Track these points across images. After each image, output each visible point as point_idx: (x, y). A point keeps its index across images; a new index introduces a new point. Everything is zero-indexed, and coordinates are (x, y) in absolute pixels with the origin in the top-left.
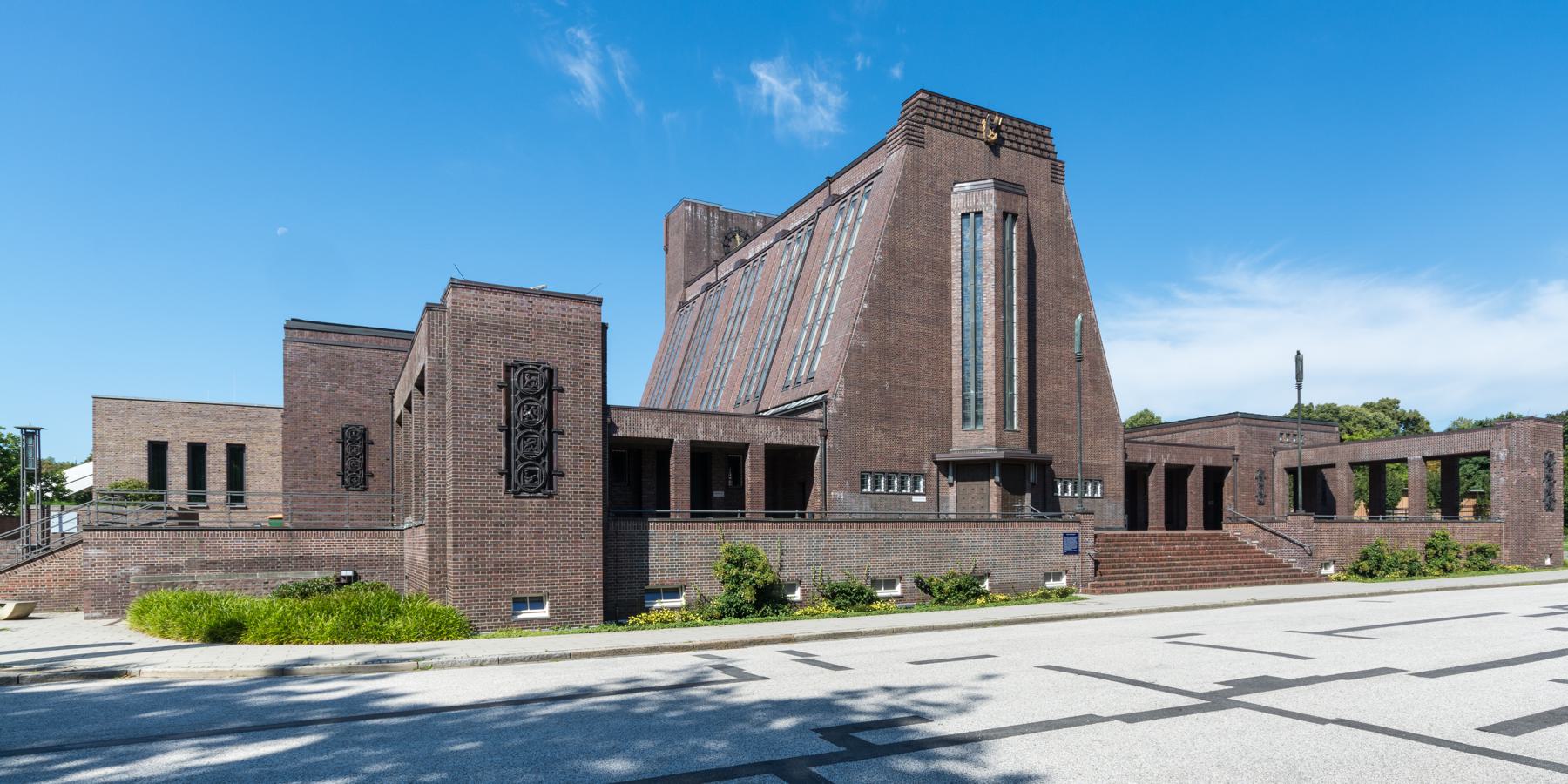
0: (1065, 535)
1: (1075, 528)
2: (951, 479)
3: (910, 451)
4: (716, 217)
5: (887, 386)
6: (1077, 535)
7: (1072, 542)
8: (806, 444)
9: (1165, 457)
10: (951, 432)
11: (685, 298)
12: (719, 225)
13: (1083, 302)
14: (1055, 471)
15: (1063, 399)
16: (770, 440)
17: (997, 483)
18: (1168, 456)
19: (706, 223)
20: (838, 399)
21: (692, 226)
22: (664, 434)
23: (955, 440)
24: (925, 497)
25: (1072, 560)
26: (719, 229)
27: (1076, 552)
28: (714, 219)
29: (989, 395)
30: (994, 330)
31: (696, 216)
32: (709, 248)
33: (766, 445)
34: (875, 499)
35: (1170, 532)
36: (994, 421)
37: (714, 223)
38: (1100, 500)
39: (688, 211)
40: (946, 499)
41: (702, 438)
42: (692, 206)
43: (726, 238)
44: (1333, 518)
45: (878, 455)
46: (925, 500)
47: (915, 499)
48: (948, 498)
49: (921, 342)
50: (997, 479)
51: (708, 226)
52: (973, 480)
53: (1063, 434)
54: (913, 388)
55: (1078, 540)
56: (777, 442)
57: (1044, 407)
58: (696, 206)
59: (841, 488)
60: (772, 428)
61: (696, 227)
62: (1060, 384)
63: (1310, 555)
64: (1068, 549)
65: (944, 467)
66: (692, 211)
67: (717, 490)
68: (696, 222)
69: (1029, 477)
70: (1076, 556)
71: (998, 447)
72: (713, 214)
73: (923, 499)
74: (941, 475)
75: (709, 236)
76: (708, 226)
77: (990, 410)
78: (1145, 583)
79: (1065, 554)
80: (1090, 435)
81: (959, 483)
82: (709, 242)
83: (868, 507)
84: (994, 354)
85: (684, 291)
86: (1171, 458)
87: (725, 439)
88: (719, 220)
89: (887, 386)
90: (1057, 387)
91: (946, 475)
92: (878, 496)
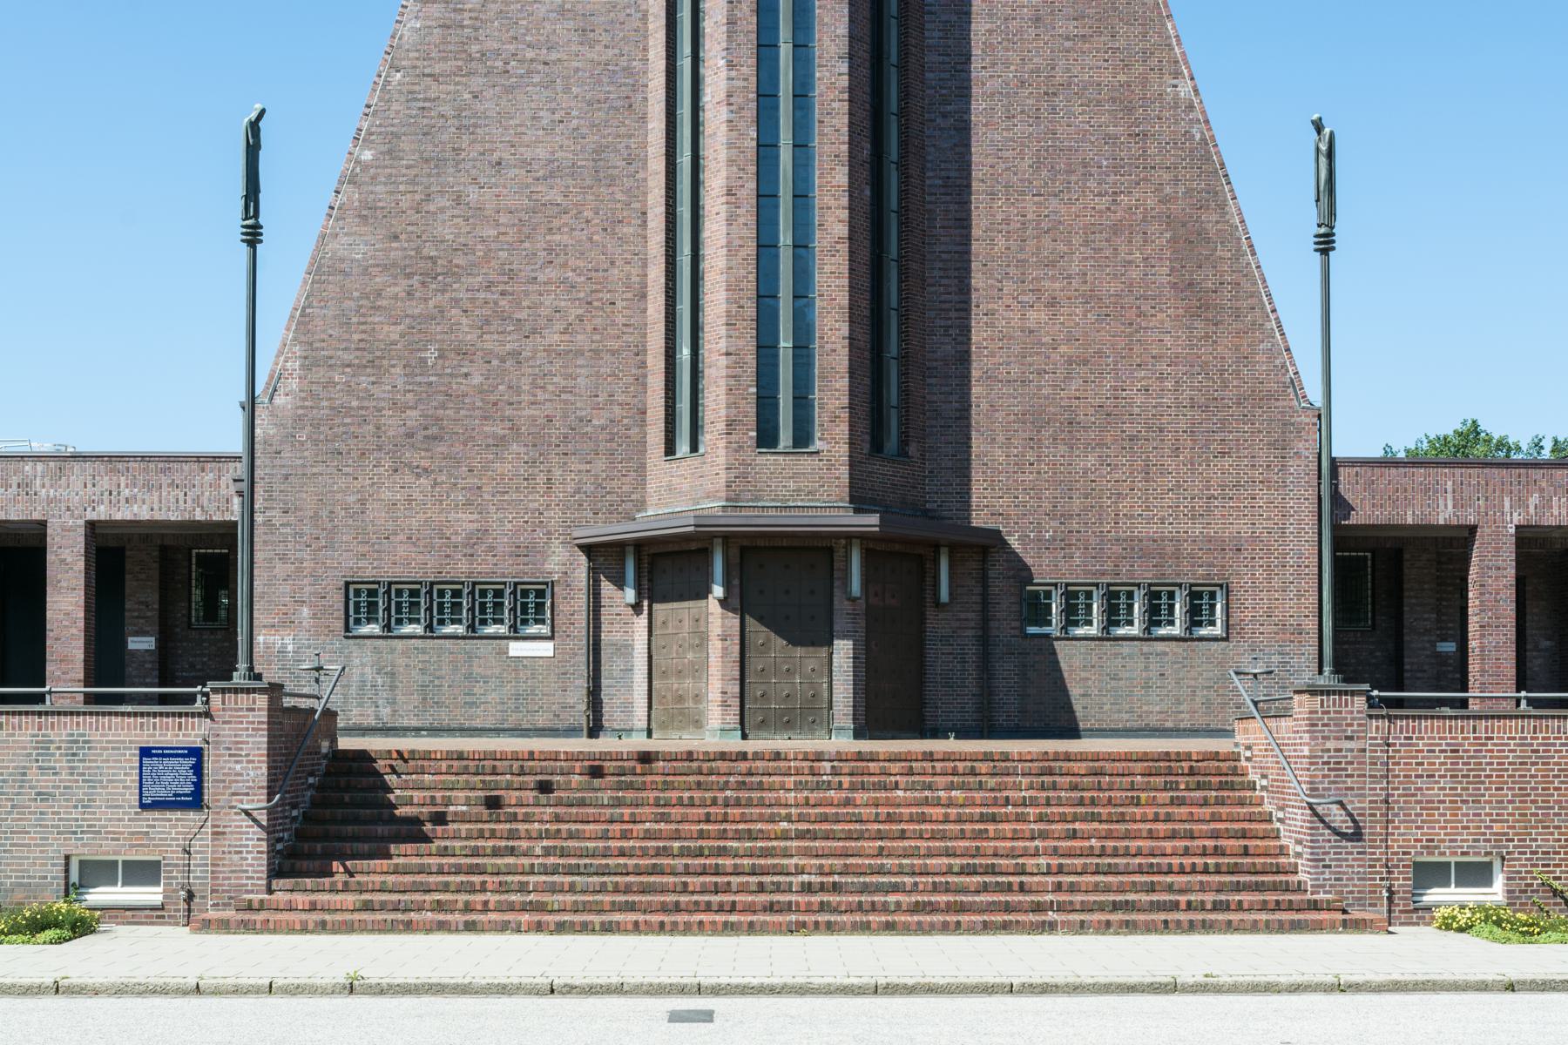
0: (145, 752)
1: (191, 733)
2: (630, 595)
3: (504, 525)
5: (431, 355)
6: (196, 753)
7: (176, 778)
8: (199, 516)
9: (1521, 503)
10: (643, 466)
13: (1146, 55)
14: (1029, 561)
15: (1063, 349)
16: (102, 513)
17: (724, 603)
18: (1534, 500)
20: (279, 400)
23: (651, 486)
25: (176, 824)
27: (195, 801)
30: (724, 173)
33: (91, 526)
34: (393, 650)
35: (867, 746)
36: (722, 426)
38: (1214, 645)
40: (625, 649)
44: (40, 699)
45: (401, 537)
47: (517, 649)
49: (543, 229)
50: (718, 591)
52: (681, 598)
53: (1063, 449)
54: (515, 354)
55: (198, 769)
56: (123, 514)
57: (990, 377)
59: (287, 622)
62: (1053, 303)
63: (1357, 835)
64: (155, 792)
67: (137, 634)
70: (192, 815)
71: (733, 502)
73: (545, 649)
74: (607, 588)
78: (439, 906)
79: (143, 806)
81: (656, 606)
83: (368, 670)
84: (723, 242)
86: (1546, 504)
89: (431, 355)
90: (1036, 316)
91: (620, 583)
92: (399, 644)
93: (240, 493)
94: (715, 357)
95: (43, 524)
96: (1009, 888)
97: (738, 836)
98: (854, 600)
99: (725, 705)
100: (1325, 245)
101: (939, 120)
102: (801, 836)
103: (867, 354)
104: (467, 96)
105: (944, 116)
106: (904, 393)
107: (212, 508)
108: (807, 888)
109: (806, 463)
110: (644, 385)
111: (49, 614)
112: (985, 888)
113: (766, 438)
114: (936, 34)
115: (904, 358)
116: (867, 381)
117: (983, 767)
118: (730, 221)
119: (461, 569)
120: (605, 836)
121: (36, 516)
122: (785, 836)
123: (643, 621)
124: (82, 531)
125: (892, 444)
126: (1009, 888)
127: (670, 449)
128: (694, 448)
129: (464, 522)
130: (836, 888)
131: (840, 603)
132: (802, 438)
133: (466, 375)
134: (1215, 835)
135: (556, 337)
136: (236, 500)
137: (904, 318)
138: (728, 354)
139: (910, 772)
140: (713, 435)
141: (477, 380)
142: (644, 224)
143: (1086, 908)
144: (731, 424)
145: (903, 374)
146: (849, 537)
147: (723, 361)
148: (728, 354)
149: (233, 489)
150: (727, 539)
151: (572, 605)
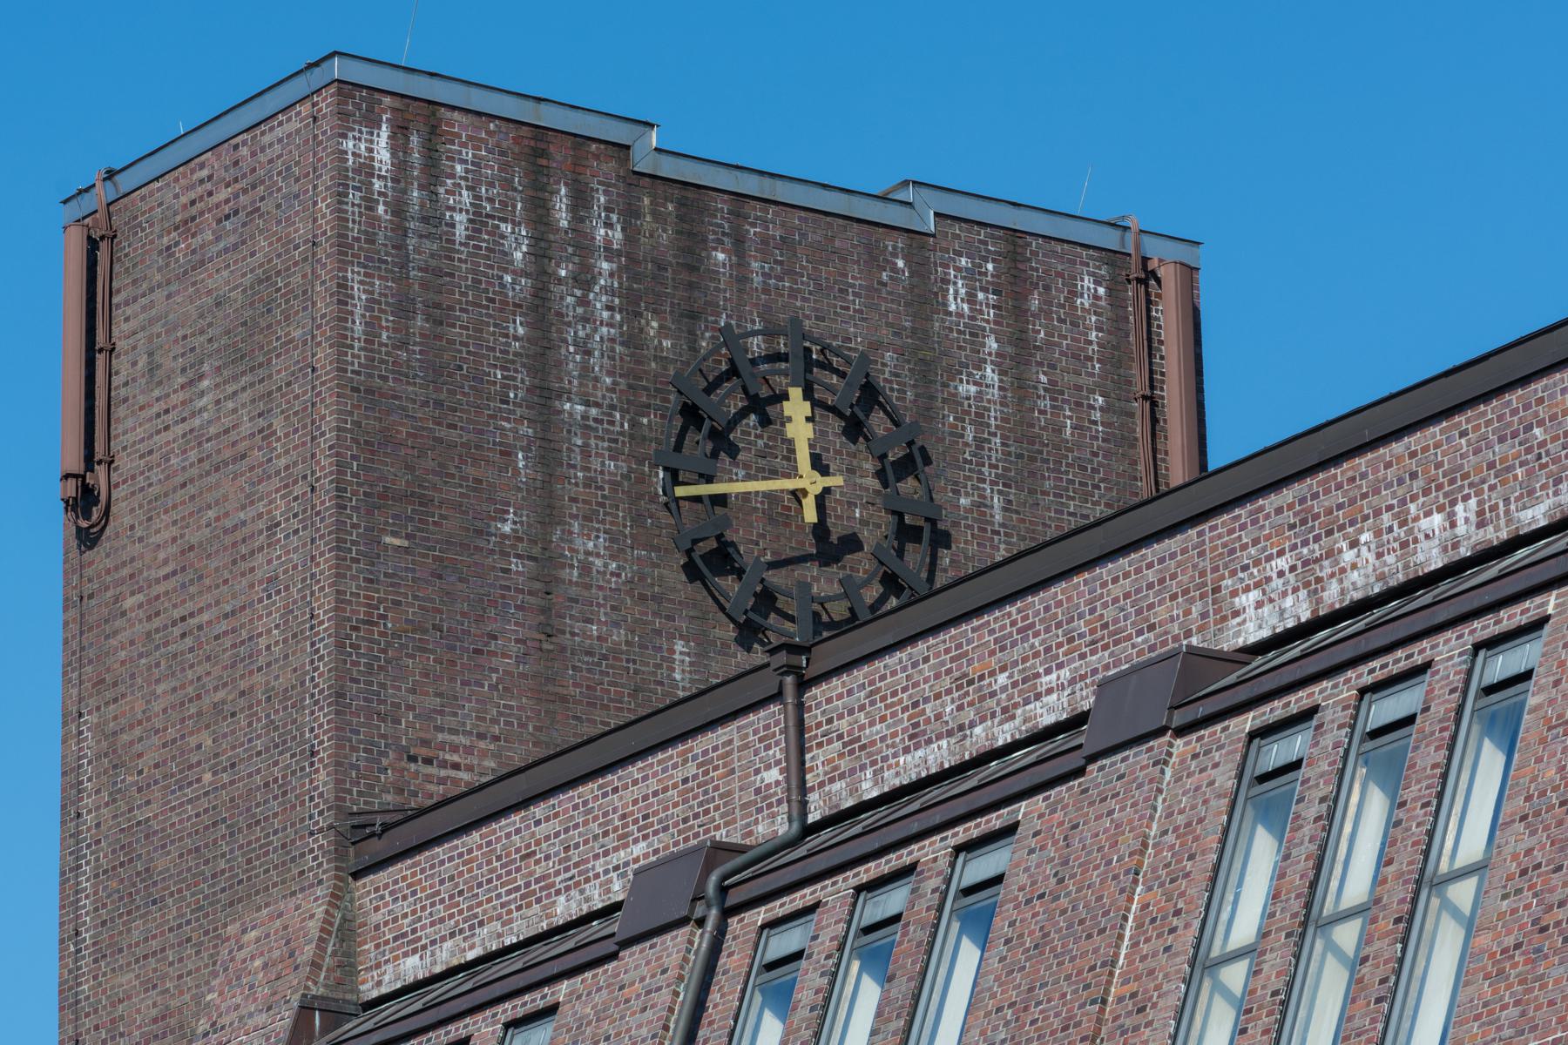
4: (610, 234)
11: (348, 967)
12: (631, 305)
19: (518, 287)
21: (404, 309)
26: (633, 340)
28: (582, 245)
31: (434, 220)
32: (548, 514)
37: (583, 278)
39: (366, 169)
42: (400, 131)
43: (692, 414)
51: (540, 308)
58: (433, 133)
61: (439, 316)
66: (401, 166)
68: (437, 274)
72: (580, 201)
75: (544, 397)
76: (540, 308)
82: (548, 454)
85: (336, 897)
88: (629, 258)
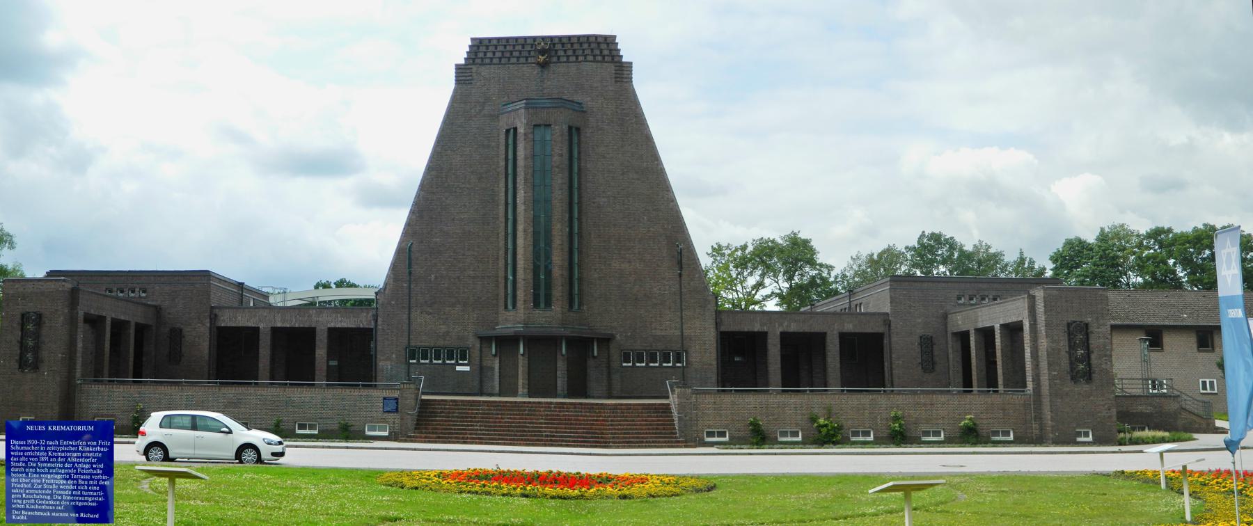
8: (361, 326)
16: (332, 325)
22: (251, 324)
24: (469, 367)
29: (520, 280)
33: (330, 329)
41: (279, 325)
46: (469, 370)
47: (458, 368)
48: (494, 368)
54: (458, 278)
56: (339, 325)
59: (388, 359)
60: (334, 315)
65: (485, 340)
69: (561, 349)
71: (526, 323)
73: (467, 368)
77: (558, 292)
80: (670, 308)
87: (297, 326)
93: (374, 320)
94: (520, 280)
95: (315, 328)
96: (598, 438)
97: (529, 423)
98: (563, 355)
99: (523, 387)
100: (680, 275)
101: (592, 204)
102: (545, 423)
103: (567, 280)
104: (444, 199)
105: (594, 203)
106: (580, 290)
107: (365, 323)
108: (547, 436)
109: (548, 313)
110: (498, 287)
111: (317, 355)
112: (592, 437)
113: (536, 305)
114: (591, 177)
115: (580, 279)
116: (568, 288)
117: (595, 407)
118: (525, 239)
119: (441, 343)
120: (495, 422)
121: (313, 326)
122: (541, 423)
123: (497, 360)
124: (326, 330)
125: (576, 306)
126: (598, 438)
127: (506, 307)
128: (514, 308)
129: (443, 328)
130: (554, 436)
131: (559, 356)
132: (548, 304)
133: (443, 284)
134: (658, 425)
135: (471, 272)
136: (373, 322)
137: (579, 266)
138: (524, 280)
139: (575, 408)
140: (520, 304)
141: (446, 285)
142: (498, 238)
143: (619, 442)
144: (525, 301)
145: (580, 284)
146: (562, 336)
147: (523, 282)
148: (524, 280)
149: (372, 318)
150: (524, 336)
151: (476, 353)
